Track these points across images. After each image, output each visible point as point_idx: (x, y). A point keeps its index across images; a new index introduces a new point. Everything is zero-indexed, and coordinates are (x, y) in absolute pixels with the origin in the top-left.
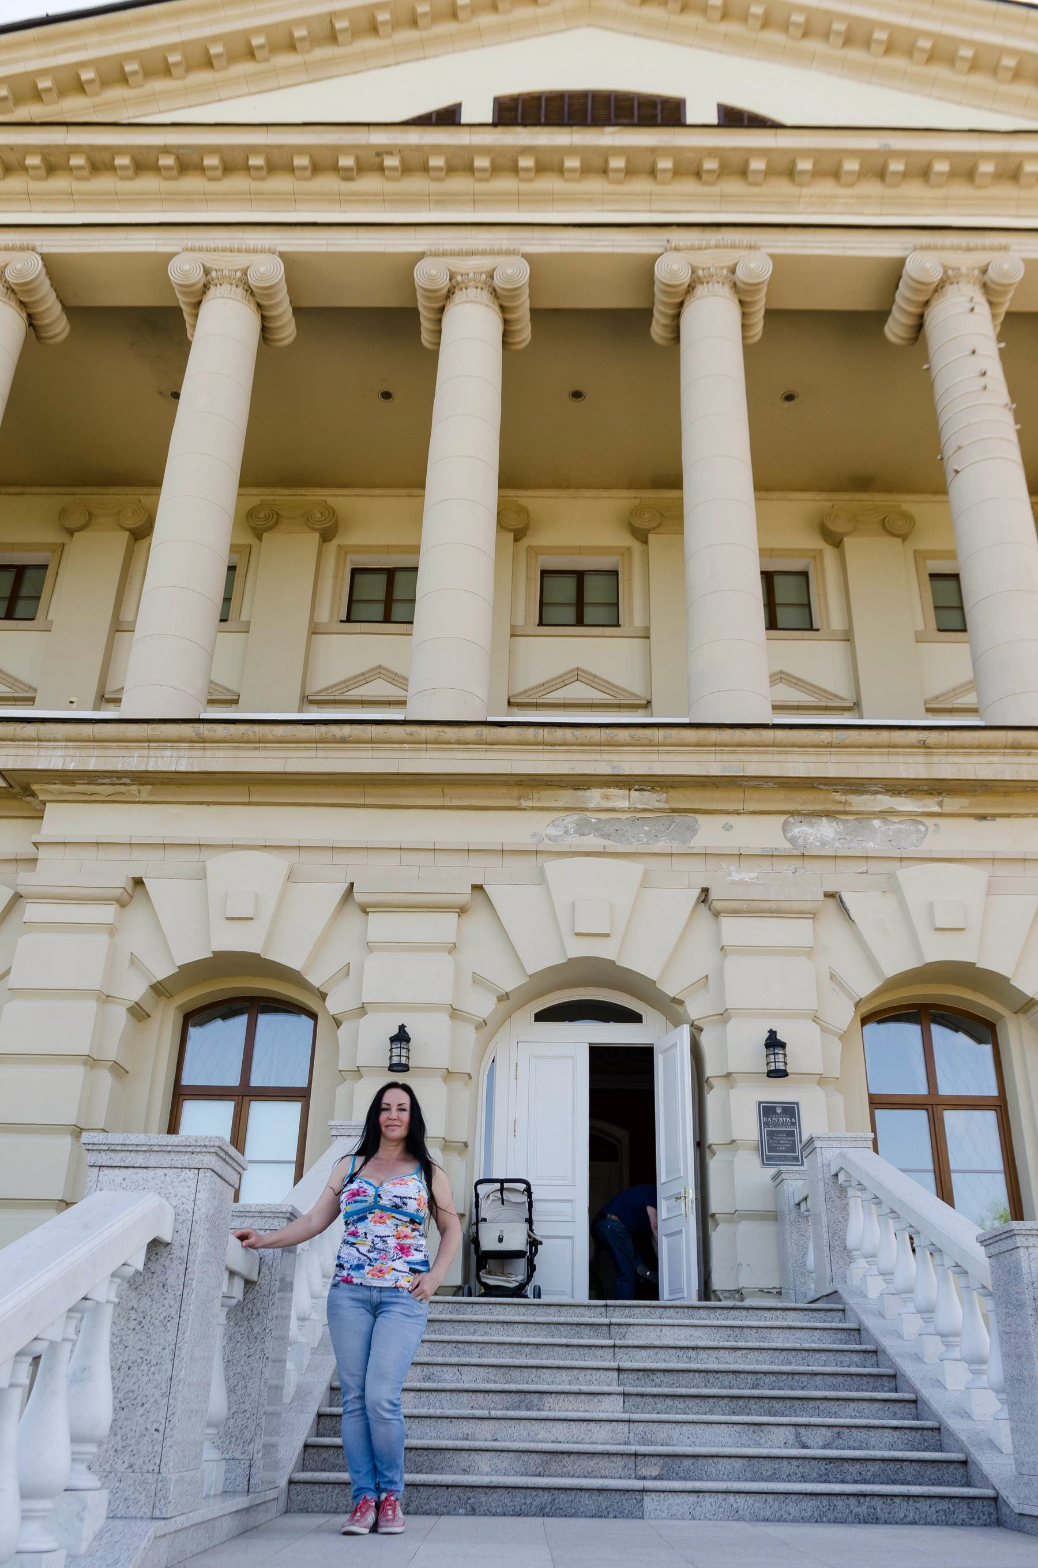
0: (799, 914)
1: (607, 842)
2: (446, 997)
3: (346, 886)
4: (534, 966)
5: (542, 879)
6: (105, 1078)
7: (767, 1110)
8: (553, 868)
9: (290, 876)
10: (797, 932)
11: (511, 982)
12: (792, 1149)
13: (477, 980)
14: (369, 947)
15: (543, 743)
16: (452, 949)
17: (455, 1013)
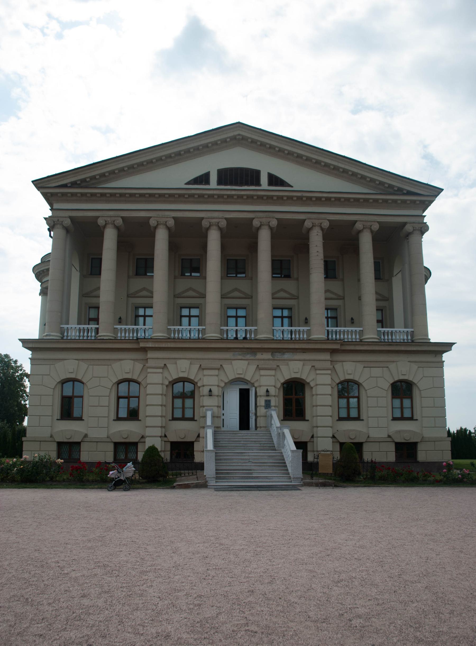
0: (273, 369)
1: (243, 357)
2: (217, 384)
3: (199, 365)
4: (230, 379)
5: (231, 364)
6: (164, 397)
7: (266, 401)
8: (234, 362)
9: (191, 364)
10: (272, 372)
11: (227, 381)
12: (269, 407)
13: (221, 380)
14: (204, 376)
15: (232, 342)
16: (217, 376)
17: (218, 386)
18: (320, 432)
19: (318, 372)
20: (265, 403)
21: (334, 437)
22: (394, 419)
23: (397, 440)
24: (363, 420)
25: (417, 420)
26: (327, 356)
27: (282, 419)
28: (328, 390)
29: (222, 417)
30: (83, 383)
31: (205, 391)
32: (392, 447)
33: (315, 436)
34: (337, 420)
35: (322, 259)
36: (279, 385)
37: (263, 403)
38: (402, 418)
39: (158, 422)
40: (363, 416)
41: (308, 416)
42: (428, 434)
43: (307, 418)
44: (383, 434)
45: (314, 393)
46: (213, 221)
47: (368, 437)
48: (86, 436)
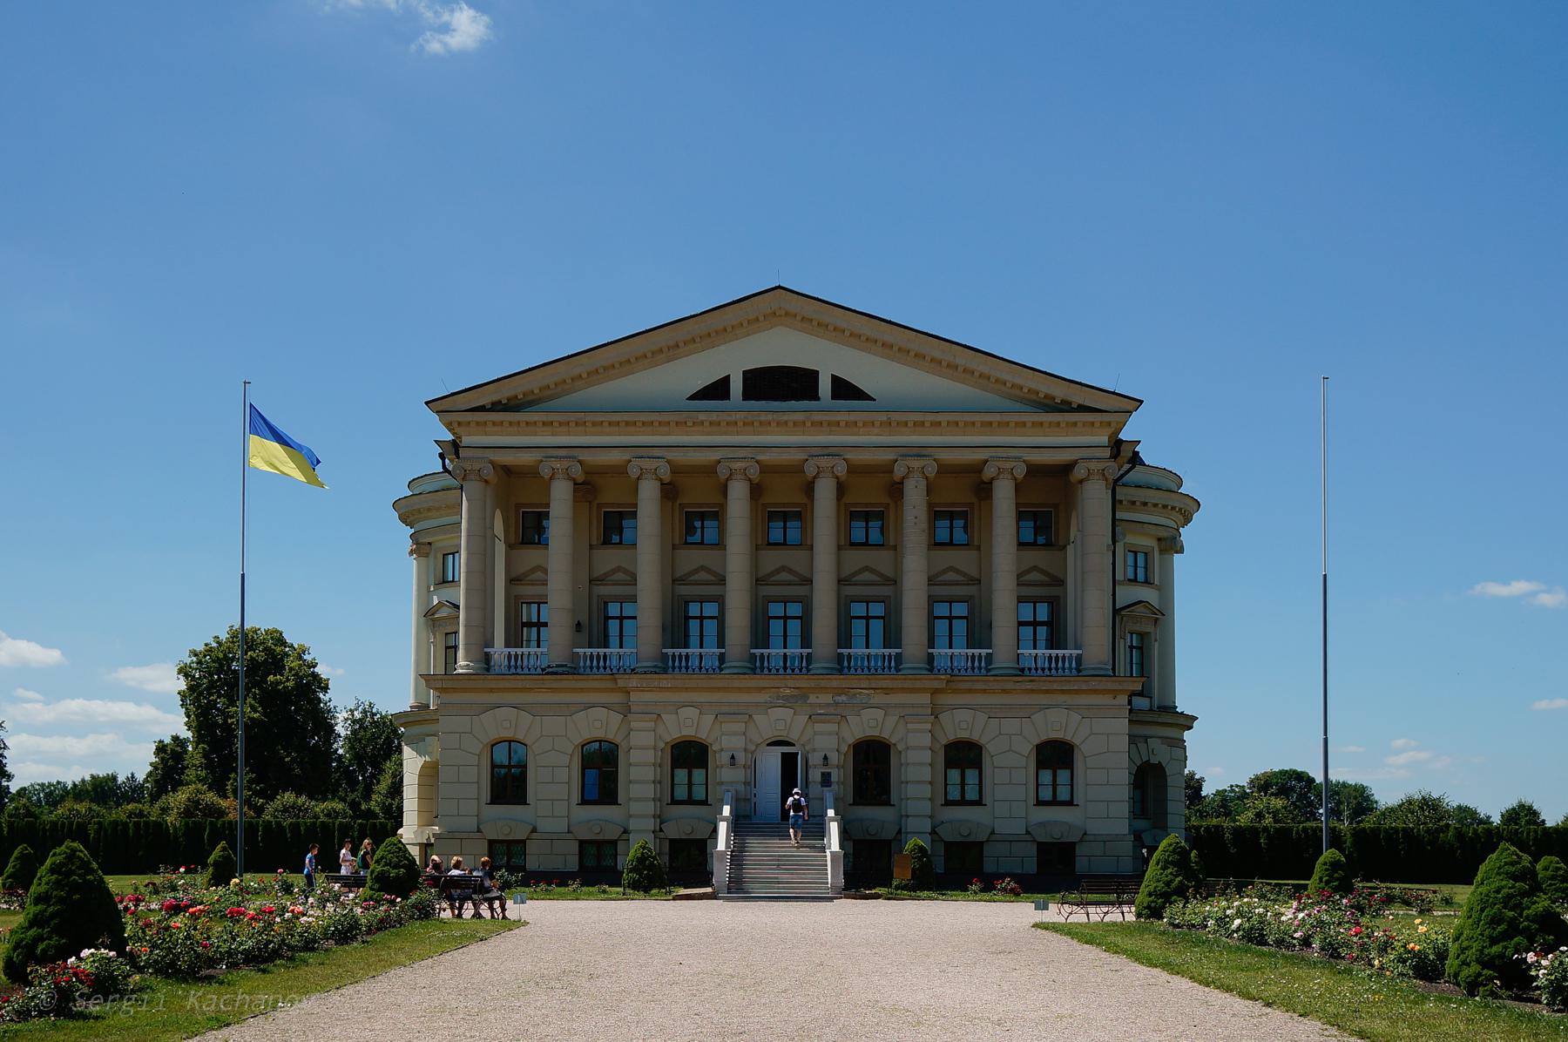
7: (823, 774)
18: (911, 824)
19: (910, 726)
20: (822, 777)
21: (933, 832)
22: (1039, 803)
23: (1040, 840)
24: (985, 805)
25: (1077, 805)
26: (925, 698)
27: (851, 802)
28: (927, 756)
29: (753, 800)
30: (526, 745)
31: (725, 758)
32: (1033, 850)
33: (903, 831)
34: (942, 805)
35: (924, 531)
36: (844, 748)
37: (818, 778)
38: (1054, 802)
39: (650, 808)
40: (987, 799)
41: (894, 798)
42: (1095, 828)
43: (892, 803)
44: (1017, 828)
45: (903, 761)
46: (737, 465)
47: (993, 833)
48: (534, 830)
